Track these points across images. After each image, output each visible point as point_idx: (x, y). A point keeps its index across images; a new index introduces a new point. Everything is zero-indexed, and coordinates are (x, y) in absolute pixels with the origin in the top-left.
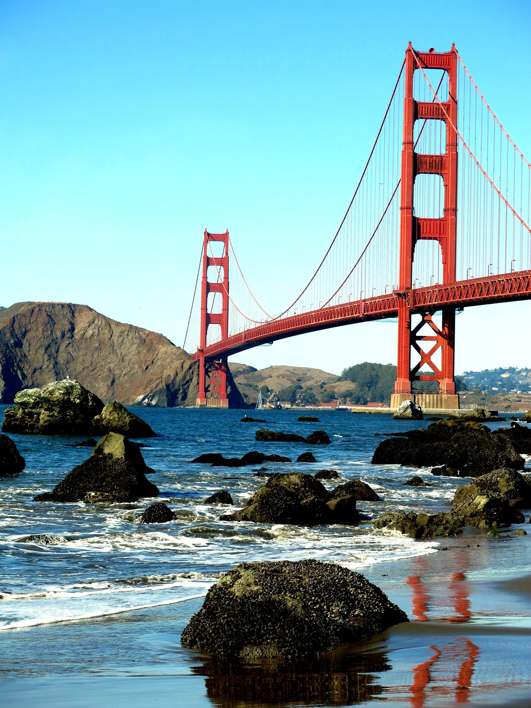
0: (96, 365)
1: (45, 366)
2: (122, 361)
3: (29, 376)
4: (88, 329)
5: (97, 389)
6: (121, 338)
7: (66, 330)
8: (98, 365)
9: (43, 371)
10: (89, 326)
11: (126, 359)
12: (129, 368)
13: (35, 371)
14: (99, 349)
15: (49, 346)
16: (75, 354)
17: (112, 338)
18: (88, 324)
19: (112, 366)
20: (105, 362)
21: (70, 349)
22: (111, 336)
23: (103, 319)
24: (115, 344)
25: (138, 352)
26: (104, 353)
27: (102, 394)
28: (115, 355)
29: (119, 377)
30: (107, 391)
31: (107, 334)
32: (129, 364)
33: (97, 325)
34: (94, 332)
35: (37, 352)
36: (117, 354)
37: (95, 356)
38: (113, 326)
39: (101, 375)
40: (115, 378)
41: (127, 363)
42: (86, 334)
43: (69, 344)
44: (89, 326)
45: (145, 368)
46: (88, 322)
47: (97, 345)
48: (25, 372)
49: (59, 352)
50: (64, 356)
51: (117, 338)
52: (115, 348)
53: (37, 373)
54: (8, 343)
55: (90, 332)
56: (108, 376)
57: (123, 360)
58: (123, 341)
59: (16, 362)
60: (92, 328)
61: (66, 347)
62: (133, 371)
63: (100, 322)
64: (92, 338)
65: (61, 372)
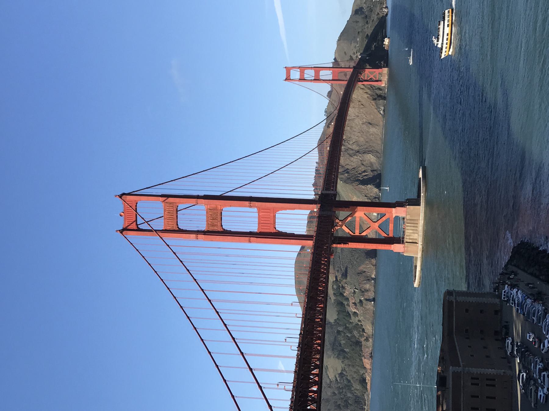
0: (360, 130)
1: (360, 158)
2: (358, 117)
3: (366, 169)
8: (360, 129)
9: (363, 160)
11: (357, 114)
12: (362, 114)
13: (363, 164)
15: (349, 154)
16: (354, 141)
19: (361, 122)
25: (353, 107)
26: (354, 125)
28: (355, 120)
32: (360, 114)
35: (352, 161)
37: (355, 130)
40: (368, 122)
41: (359, 114)
45: (362, 106)
48: (363, 170)
49: (352, 148)
52: (351, 119)
53: (364, 163)
54: (347, 178)
56: (367, 125)
57: (358, 116)
59: (358, 175)
62: (364, 112)
65: (364, 150)
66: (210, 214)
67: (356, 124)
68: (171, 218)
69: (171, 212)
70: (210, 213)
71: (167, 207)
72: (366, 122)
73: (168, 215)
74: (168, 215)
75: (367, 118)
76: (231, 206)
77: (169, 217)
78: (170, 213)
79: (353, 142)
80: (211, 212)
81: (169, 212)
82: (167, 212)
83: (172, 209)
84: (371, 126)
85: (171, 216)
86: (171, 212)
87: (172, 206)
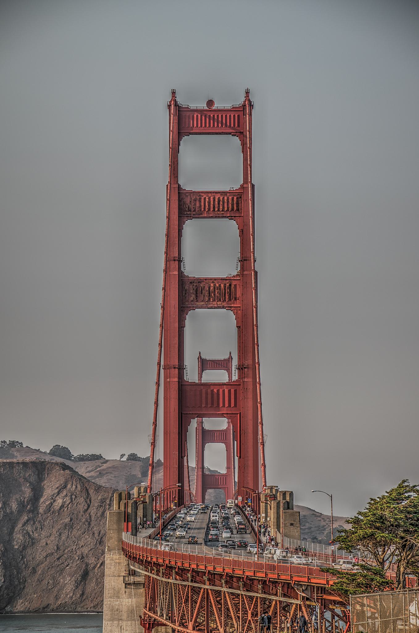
0: (64, 551)
2: (100, 543)
4: (58, 498)
5: (61, 586)
6: (101, 510)
7: (26, 499)
10: (58, 493)
14: (70, 526)
17: (89, 511)
18: (57, 491)
19: (85, 550)
20: (76, 545)
21: (29, 528)
22: (89, 506)
23: (78, 482)
24: (93, 518)
26: (76, 532)
27: (67, 595)
29: (94, 567)
30: (74, 590)
31: (83, 505)
33: (70, 490)
34: (65, 502)
36: (94, 533)
38: (91, 492)
39: (70, 566)
42: (54, 504)
43: (28, 521)
44: (58, 493)
46: (57, 488)
47: (67, 520)
50: (19, 538)
51: (95, 510)
55: (59, 501)
58: (103, 513)
60: (63, 495)
61: (23, 526)
63: (74, 487)
64: (62, 510)
66: (220, 286)
67: (79, 538)
68: (209, 206)
69: (221, 207)
70: (222, 286)
71: (230, 197)
72: (87, 565)
73: (214, 200)
74: (214, 200)
75: (98, 566)
76: (238, 327)
77: (209, 202)
78: (219, 204)
79: (31, 533)
80: (225, 287)
81: (221, 203)
82: (221, 198)
83: (228, 208)
84: (79, 578)
85: (212, 206)
86: (221, 207)
87: (233, 210)
